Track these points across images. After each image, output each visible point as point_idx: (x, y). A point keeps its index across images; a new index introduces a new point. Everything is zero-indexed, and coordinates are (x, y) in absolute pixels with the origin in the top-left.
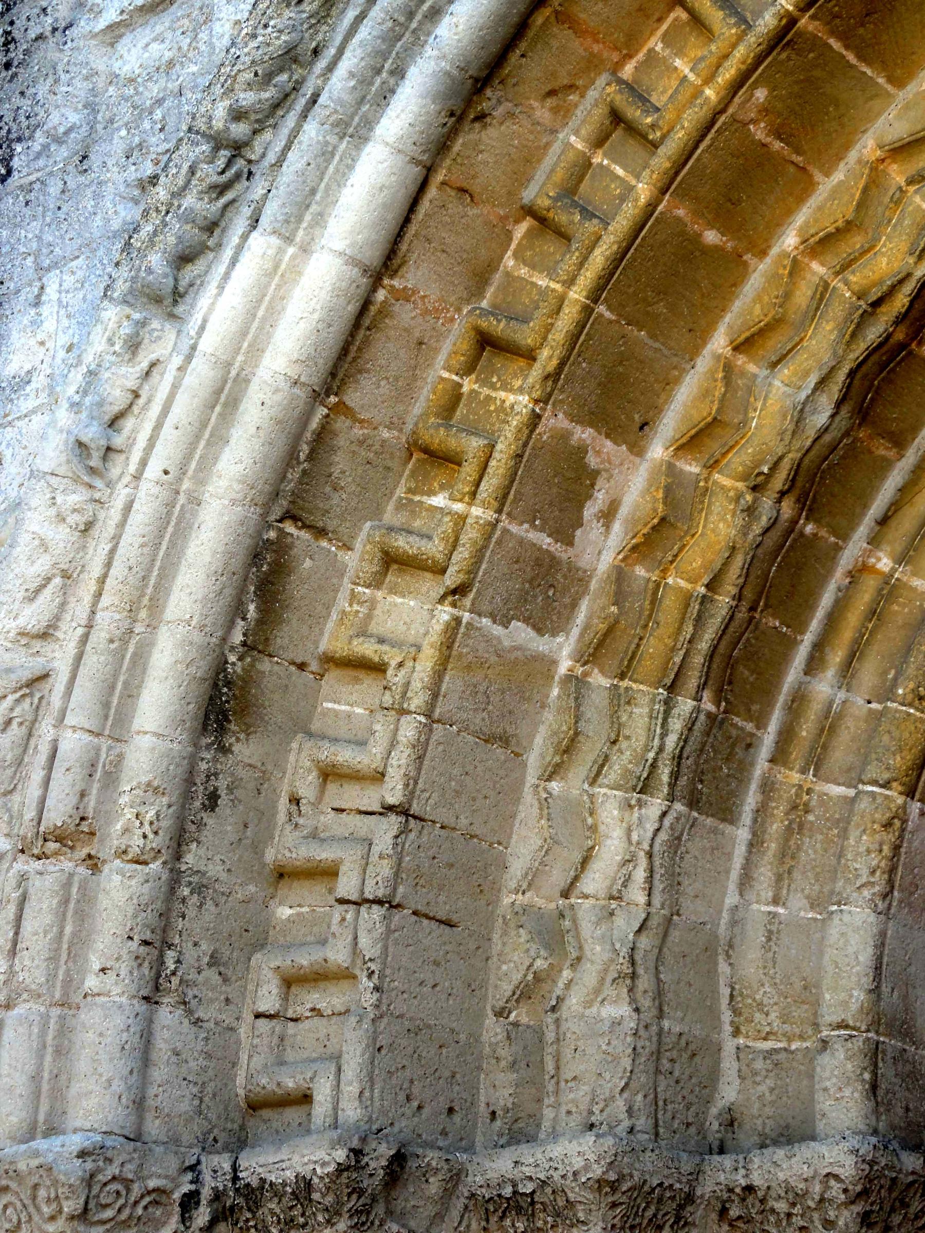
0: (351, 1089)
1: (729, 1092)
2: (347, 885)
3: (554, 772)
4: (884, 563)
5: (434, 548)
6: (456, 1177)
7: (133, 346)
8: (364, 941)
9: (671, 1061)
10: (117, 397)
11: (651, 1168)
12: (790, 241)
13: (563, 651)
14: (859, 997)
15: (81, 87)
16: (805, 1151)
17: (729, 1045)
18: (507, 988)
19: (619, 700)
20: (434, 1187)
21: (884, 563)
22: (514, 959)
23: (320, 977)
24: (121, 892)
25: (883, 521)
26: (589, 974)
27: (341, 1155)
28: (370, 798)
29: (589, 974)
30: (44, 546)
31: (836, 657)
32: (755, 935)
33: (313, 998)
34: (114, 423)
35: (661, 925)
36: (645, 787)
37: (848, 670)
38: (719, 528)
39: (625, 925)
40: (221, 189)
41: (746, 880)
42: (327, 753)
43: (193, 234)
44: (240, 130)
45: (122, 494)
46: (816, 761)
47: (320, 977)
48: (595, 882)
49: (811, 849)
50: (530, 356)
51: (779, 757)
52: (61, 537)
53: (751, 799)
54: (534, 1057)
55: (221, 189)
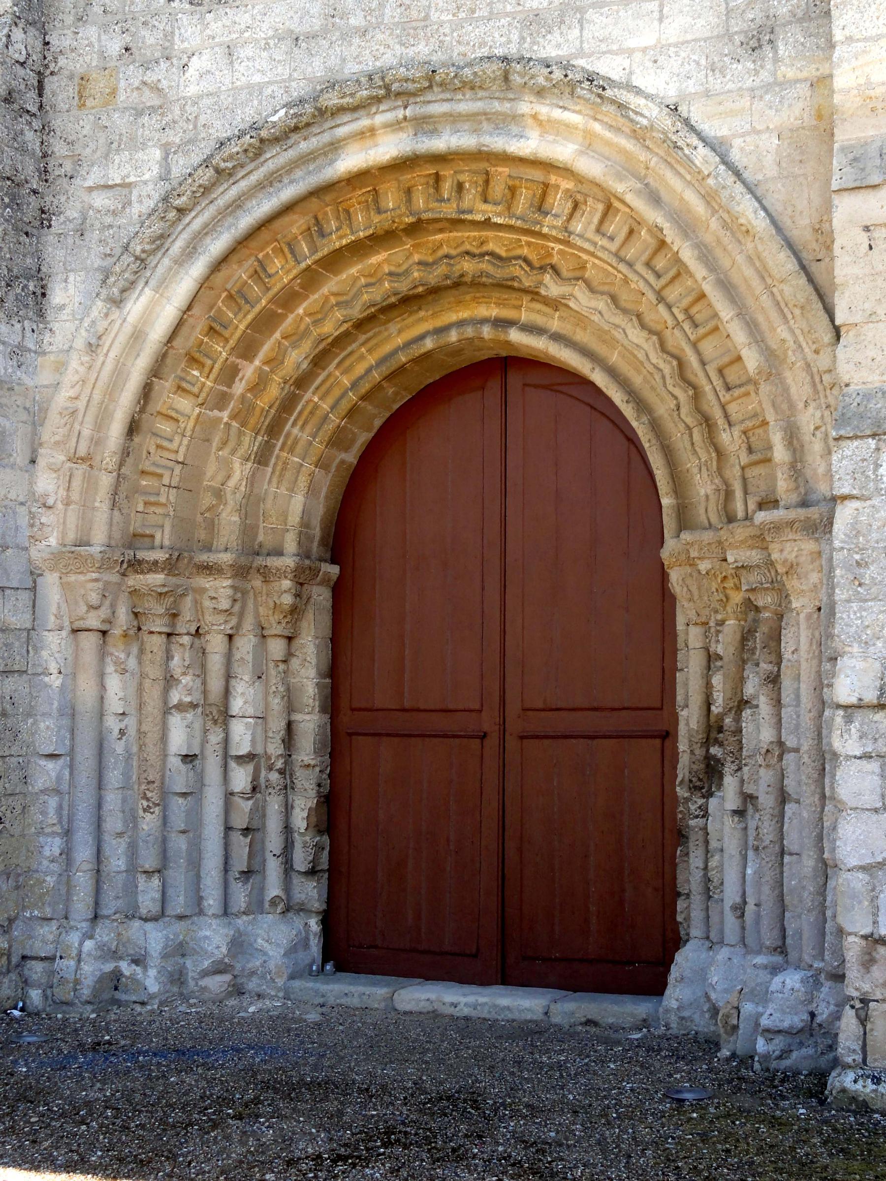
0: (167, 536)
1: (261, 538)
2: (166, 481)
3: (220, 449)
4: (316, 399)
5: (195, 390)
6: (191, 558)
7: (107, 315)
8: (171, 498)
9: (248, 530)
10: (101, 330)
11: (243, 561)
12: (301, 311)
13: (225, 415)
14: (298, 519)
15: (78, 205)
16: (282, 559)
17: (261, 526)
18: (204, 508)
19: (240, 434)
20: (186, 561)
21: (316, 399)
22: (207, 500)
23: (157, 504)
24: (106, 481)
25: (317, 388)
26: (229, 509)
27: (167, 556)
28: (172, 456)
29: (229, 509)
30: (77, 372)
31: (300, 423)
32: (271, 497)
33: (152, 509)
34: (99, 338)
35: (247, 497)
36: (247, 460)
37: (303, 428)
38: (274, 391)
39: (239, 496)
40: (136, 272)
41: (270, 482)
42: (159, 441)
43: (127, 284)
44: (144, 256)
45: (101, 359)
46: (291, 451)
47: (157, 504)
48: (232, 483)
49: (288, 475)
50: (227, 340)
51: (282, 449)
52: (82, 369)
53: (273, 460)
54: (211, 526)
55: (136, 272)
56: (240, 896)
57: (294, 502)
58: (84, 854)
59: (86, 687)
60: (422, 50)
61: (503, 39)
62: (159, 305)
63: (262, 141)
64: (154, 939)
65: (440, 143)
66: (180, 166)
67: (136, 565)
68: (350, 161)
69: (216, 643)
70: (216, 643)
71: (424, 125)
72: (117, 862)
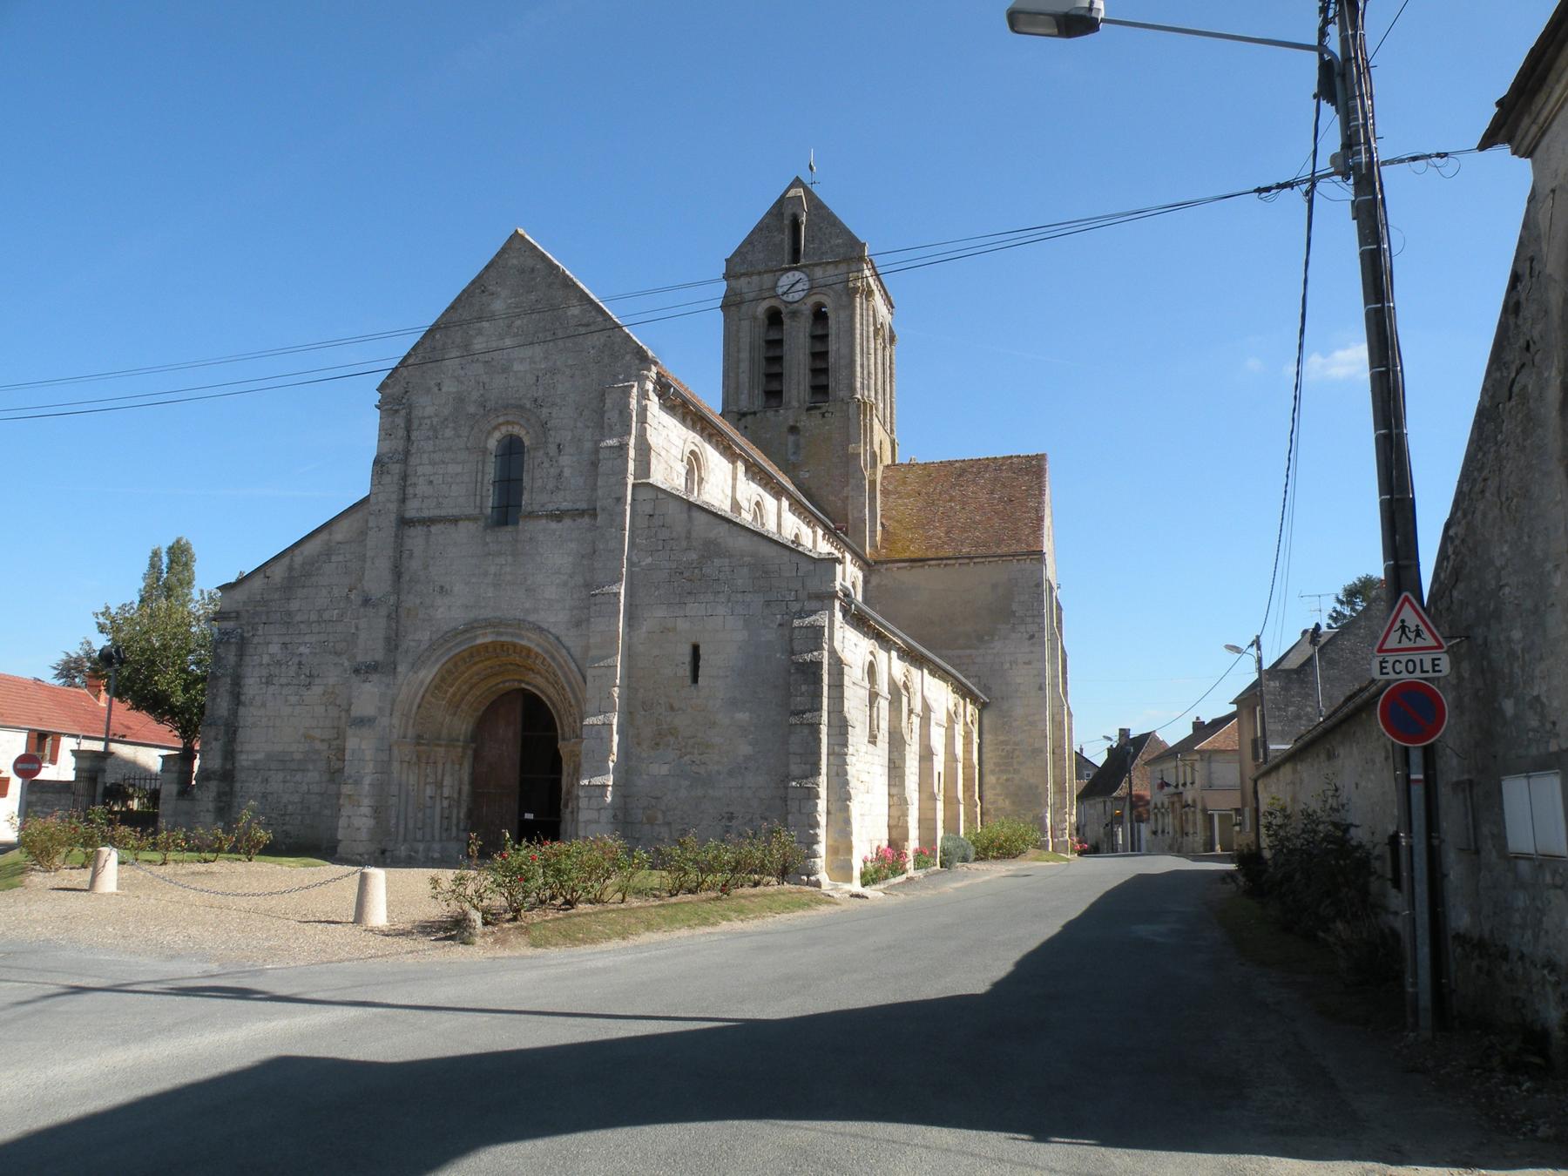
56: (445, 835)
57: (462, 726)
58: (402, 822)
59: (404, 777)
60: (499, 614)
61: (519, 615)
62: (428, 674)
63: (456, 633)
64: (421, 847)
65: (503, 639)
66: (434, 637)
67: (419, 744)
68: (479, 641)
69: (440, 767)
70: (440, 767)
71: (501, 634)
72: (411, 826)
